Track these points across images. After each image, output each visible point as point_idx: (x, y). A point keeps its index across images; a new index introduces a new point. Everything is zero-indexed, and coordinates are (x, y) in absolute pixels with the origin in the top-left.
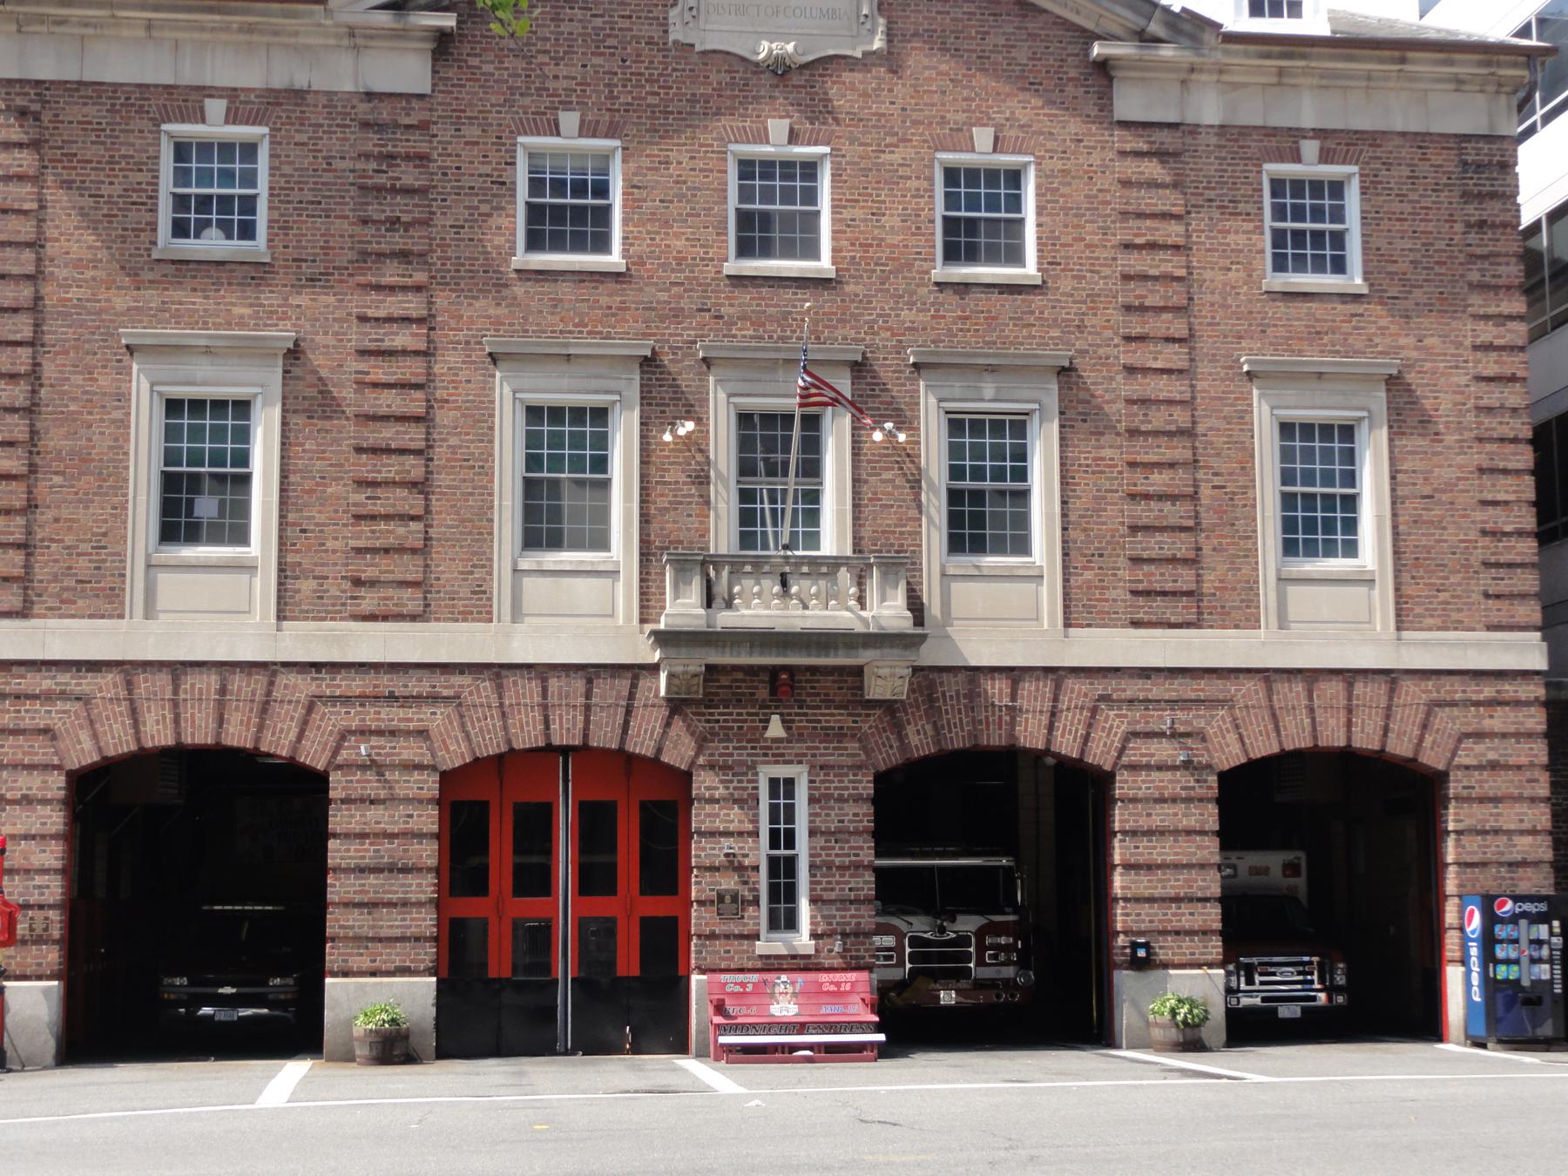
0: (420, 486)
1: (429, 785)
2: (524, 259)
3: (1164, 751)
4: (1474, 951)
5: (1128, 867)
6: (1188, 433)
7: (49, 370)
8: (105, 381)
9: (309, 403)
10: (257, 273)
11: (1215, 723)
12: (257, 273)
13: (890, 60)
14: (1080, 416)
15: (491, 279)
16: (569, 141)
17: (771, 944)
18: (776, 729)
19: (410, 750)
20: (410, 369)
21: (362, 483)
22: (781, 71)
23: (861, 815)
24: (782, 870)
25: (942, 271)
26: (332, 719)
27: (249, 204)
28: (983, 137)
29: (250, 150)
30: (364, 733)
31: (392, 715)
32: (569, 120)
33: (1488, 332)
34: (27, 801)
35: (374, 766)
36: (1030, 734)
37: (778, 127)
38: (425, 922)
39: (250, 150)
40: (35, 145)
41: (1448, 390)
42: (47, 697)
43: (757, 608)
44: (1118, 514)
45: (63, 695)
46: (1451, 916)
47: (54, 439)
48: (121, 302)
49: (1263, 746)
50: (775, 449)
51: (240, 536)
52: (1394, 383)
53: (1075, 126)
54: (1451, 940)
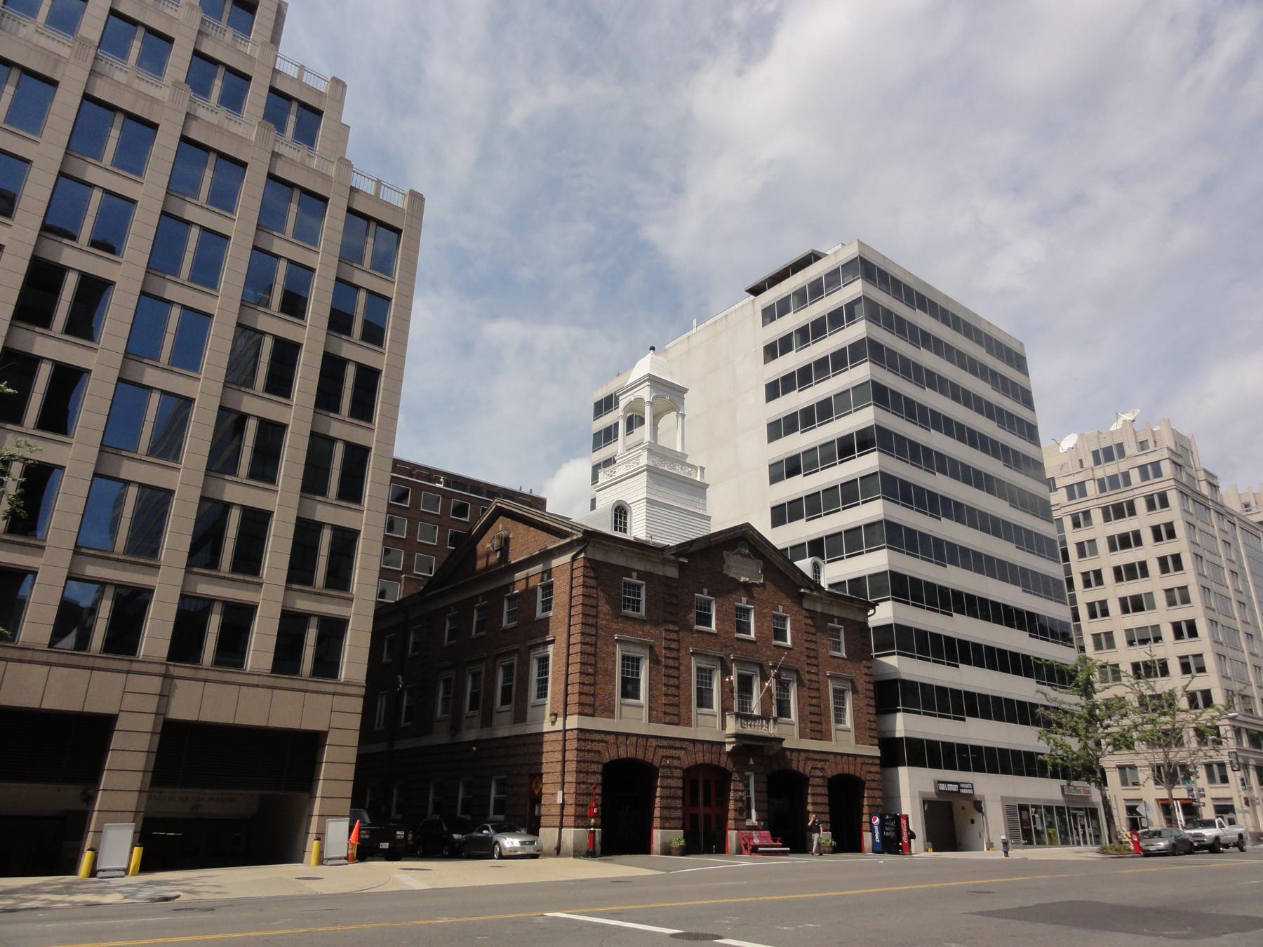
0: (677, 687)
1: (678, 773)
2: (697, 627)
3: (818, 773)
4: (876, 828)
5: (813, 804)
6: (818, 690)
7: (599, 644)
8: (611, 649)
9: (655, 661)
10: (641, 621)
11: (827, 765)
12: (641, 621)
13: (763, 585)
14: (800, 683)
15: (690, 630)
16: (704, 596)
17: (748, 823)
18: (751, 762)
19: (676, 763)
20: (674, 654)
21: (665, 685)
22: (745, 583)
23: (764, 787)
24: (749, 799)
25: (775, 642)
26: (661, 752)
27: (638, 602)
28: (781, 608)
29: (639, 587)
30: (667, 757)
31: (673, 752)
32: (705, 591)
33: (866, 671)
34: (594, 773)
35: (669, 767)
36: (794, 766)
37: (744, 599)
38: (679, 813)
39: (639, 587)
40: (596, 578)
41: (861, 686)
42: (599, 741)
43: (750, 730)
44: (808, 709)
45: (602, 741)
46: (865, 818)
47: (600, 665)
48: (615, 626)
49: (835, 773)
50: (745, 684)
51: (637, 697)
52: (852, 681)
53: (796, 608)
54: (866, 826)
